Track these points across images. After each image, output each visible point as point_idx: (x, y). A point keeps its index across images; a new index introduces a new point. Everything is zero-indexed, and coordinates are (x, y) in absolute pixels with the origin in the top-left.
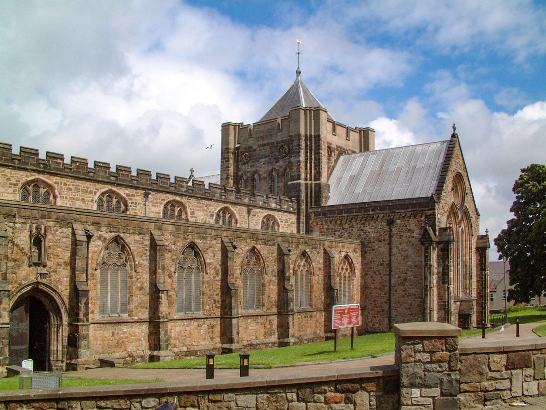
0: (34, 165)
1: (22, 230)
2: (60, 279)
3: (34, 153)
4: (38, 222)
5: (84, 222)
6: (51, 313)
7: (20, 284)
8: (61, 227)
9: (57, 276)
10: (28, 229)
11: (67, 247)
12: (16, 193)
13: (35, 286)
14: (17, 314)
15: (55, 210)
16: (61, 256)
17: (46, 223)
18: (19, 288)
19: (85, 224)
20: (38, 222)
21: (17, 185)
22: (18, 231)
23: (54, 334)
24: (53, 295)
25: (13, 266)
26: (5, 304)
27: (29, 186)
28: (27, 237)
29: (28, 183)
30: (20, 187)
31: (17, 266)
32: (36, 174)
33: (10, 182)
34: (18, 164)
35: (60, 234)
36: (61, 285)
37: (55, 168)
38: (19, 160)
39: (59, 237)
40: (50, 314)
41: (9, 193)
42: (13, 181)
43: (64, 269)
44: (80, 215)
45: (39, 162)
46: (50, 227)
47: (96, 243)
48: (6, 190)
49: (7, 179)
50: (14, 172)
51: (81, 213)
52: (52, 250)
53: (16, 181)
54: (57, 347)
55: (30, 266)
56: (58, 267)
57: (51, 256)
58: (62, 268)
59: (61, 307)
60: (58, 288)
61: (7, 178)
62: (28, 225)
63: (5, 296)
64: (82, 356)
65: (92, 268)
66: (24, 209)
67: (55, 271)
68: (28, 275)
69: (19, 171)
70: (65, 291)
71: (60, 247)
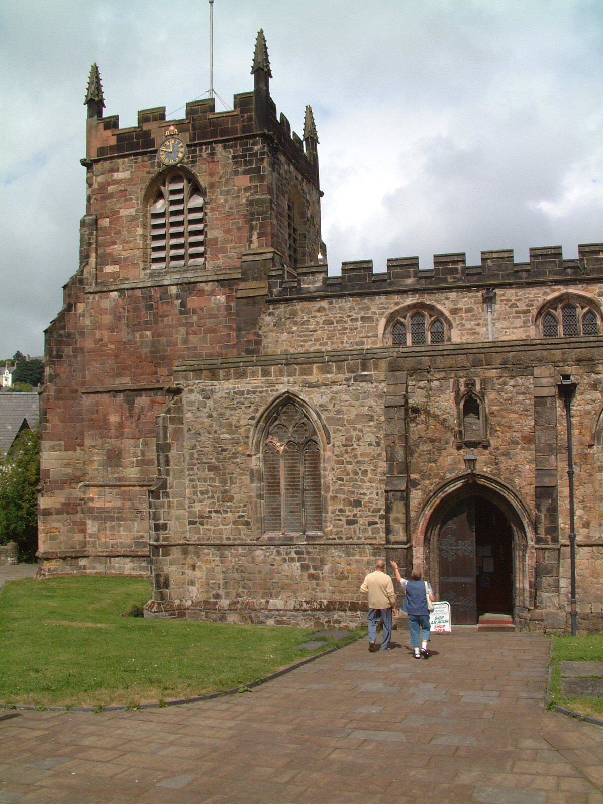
0: (556, 273)
1: (441, 390)
2: (516, 466)
3: (551, 254)
4: (468, 374)
5: (559, 361)
6: (513, 525)
7: (442, 479)
8: (512, 377)
9: (509, 461)
10: (451, 388)
11: (527, 410)
12: (529, 325)
13: (470, 481)
14: (454, 527)
15: (499, 349)
16: (517, 427)
17: (484, 373)
18: (440, 486)
19: (561, 364)
20: (468, 374)
21: (528, 311)
22: (434, 392)
23: (519, 561)
24: (505, 495)
25: (430, 450)
26: (398, 512)
27: (555, 309)
28: (451, 401)
29: (553, 303)
30: (535, 313)
31: (437, 450)
32: (561, 287)
33: (516, 309)
34: (526, 278)
35: (511, 389)
36: (520, 476)
37: (592, 271)
38: (527, 271)
39: (509, 395)
40: (511, 527)
41: (516, 328)
42: (522, 306)
43: (523, 448)
44: (549, 349)
45: (566, 265)
46: (491, 379)
47: (588, 397)
48: (512, 323)
49: (511, 306)
50: (520, 292)
51: (552, 347)
52: (498, 418)
53: (527, 305)
54: (523, 584)
55: (459, 448)
56: (512, 446)
57: (498, 428)
58: (519, 447)
59: (521, 516)
60: (514, 482)
61: (510, 303)
62: (451, 381)
63: (396, 500)
64: (544, 605)
65: (582, 444)
66: (441, 355)
67: (506, 454)
68: (456, 463)
69: (531, 289)
70: (528, 488)
71: (514, 412)
